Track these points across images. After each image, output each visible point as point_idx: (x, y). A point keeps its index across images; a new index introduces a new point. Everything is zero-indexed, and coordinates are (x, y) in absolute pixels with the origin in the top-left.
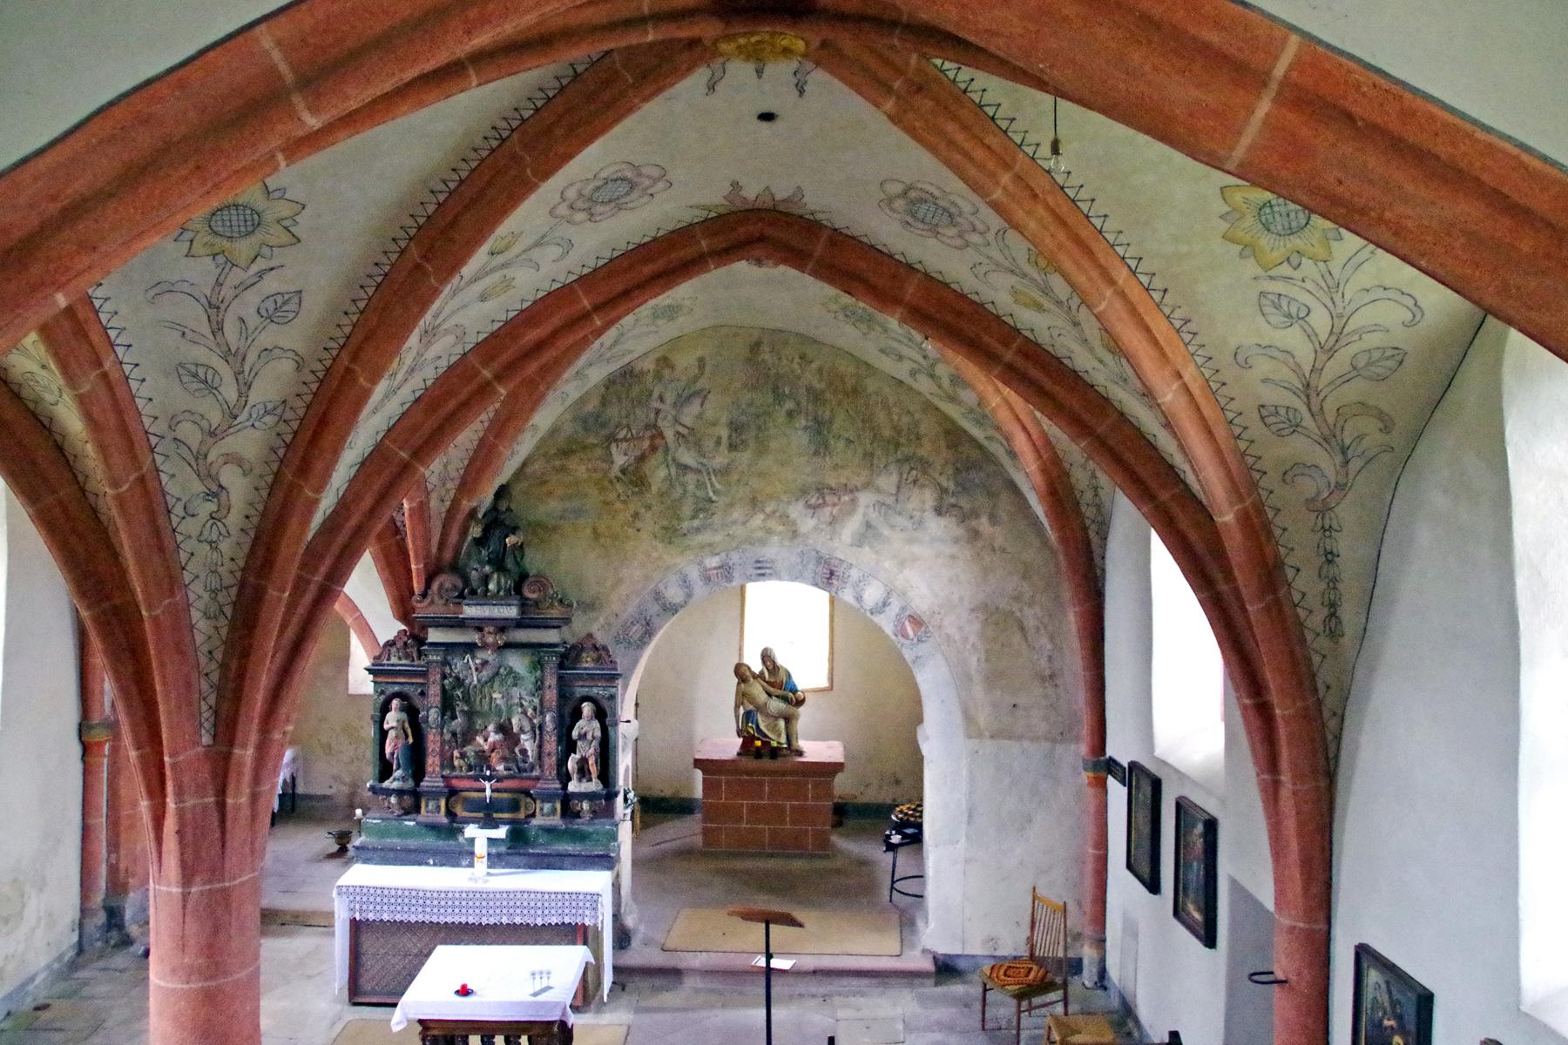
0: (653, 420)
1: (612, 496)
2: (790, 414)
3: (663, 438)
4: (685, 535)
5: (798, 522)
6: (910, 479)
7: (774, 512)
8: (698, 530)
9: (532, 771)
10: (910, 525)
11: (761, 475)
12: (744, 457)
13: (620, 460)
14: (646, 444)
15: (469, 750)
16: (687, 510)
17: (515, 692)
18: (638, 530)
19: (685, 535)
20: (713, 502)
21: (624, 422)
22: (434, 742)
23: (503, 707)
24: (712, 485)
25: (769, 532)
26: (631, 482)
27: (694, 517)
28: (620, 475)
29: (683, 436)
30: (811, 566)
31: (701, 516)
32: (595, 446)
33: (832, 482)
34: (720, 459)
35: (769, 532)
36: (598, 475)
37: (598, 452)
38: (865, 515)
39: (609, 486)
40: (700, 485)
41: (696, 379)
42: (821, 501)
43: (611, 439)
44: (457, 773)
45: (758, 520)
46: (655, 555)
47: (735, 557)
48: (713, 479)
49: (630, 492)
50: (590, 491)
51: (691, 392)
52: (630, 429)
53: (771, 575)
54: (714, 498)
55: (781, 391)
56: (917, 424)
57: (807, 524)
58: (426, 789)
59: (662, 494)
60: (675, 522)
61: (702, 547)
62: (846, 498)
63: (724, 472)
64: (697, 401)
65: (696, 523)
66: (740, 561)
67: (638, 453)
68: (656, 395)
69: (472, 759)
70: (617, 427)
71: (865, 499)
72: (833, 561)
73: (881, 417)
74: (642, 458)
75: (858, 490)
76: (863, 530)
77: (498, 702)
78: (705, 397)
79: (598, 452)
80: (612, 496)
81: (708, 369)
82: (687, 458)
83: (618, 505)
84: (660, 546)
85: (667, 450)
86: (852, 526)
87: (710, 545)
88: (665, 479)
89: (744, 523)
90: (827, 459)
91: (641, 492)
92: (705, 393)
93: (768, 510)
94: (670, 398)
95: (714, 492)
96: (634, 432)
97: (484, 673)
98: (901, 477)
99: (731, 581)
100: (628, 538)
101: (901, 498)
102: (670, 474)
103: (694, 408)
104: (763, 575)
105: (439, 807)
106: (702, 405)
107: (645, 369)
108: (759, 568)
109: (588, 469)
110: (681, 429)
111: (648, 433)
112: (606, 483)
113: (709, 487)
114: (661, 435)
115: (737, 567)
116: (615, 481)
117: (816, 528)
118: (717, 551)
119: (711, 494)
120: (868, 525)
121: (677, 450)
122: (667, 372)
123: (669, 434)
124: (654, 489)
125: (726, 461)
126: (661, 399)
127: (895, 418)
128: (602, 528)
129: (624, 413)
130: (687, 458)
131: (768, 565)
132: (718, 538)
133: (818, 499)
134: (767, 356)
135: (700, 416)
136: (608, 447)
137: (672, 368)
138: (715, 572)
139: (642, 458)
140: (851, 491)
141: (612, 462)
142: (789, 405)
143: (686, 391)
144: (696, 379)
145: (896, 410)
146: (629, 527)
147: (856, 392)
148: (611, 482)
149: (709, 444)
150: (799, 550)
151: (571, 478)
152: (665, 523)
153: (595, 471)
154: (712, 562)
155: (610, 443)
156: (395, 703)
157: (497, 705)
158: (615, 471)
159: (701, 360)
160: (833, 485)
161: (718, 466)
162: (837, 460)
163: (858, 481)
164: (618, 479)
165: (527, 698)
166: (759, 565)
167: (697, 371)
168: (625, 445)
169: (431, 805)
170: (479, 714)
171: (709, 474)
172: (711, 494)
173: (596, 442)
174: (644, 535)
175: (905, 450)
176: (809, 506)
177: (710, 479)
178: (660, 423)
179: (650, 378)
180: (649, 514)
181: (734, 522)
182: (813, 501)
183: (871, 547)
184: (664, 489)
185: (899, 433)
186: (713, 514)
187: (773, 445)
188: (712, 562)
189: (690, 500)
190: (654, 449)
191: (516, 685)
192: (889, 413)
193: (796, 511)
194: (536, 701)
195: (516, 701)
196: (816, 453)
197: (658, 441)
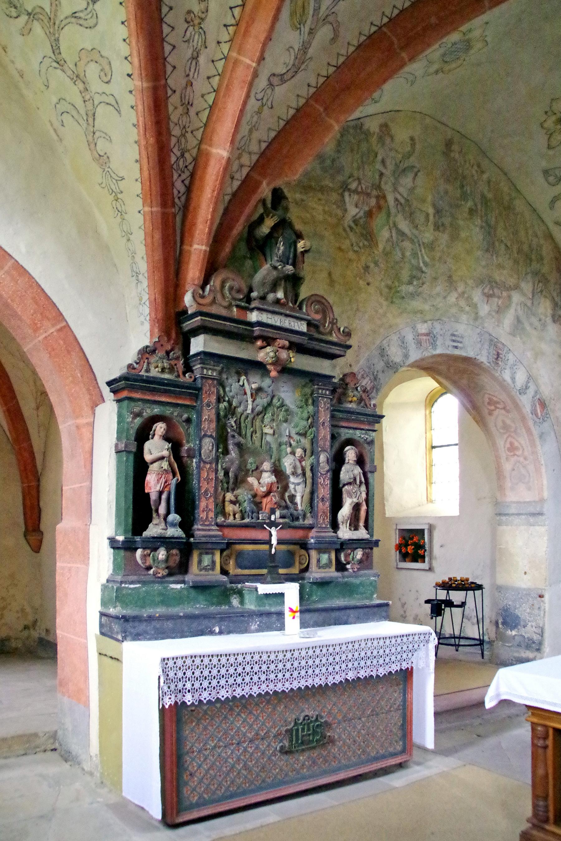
0: (377, 182)
1: (346, 244)
2: (472, 212)
3: (386, 201)
4: (403, 298)
5: (478, 305)
6: (539, 290)
7: (463, 293)
8: (413, 296)
9: (304, 520)
10: (539, 326)
11: (456, 258)
12: (444, 238)
13: (352, 211)
14: (373, 201)
15: (243, 494)
16: (405, 274)
17: (287, 429)
18: (368, 284)
19: (403, 298)
20: (423, 272)
21: (355, 174)
22: (208, 480)
23: (274, 446)
24: (423, 257)
25: (461, 310)
26: (362, 235)
27: (410, 283)
28: (353, 225)
29: (401, 204)
30: (486, 346)
31: (415, 283)
32: (332, 189)
33: (497, 278)
34: (428, 235)
35: (461, 310)
36: (333, 221)
37: (334, 196)
38: (516, 310)
39: (344, 234)
40: (415, 255)
41: (409, 155)
42: (491, 292)
43: (345, 187)
44: (231, 520)
45: (452, 298)
46: (381, 311)
47: (438, 326)
48: (423, 251)
49: (361, 244)
50: (327, 234)
51: (405, 166)
52: (360, 183)
53: (461, 348)
54: (424, 269)
55: (465, 189)
56: (541, 246)
57: (484, 309)
58: (204, 540)
59: (387, 254)
60: (397, 284)
61: (415, 312)
62: (505, 294)
63: (431, 246)
64: (411, 175)
65: (411, 289)
66: (441, 332)
67: (367, 209)
68: (380, 157)
69: (246, 504)
70: (349, 177)
71: (516, 297)
72: (499, 345)
73: (522, 233)
74: (369, 214)
75: (511, 290)
76: (516, 323)
77: (269, 438)
78: (416, 175)
79: (334, 196)
80: (346, 244)
81: (418, 147)
82: (404, 226)
83: (351, 255)
84: (385, 303)
85: (389, 214)
86: (508, 319)
87: (421, 312)
88: (388, 241)
89: (445, 298)
90: (494, 257)
91: (370, 247)
92: (416, 170)
93: (460, 290)
94: (390, 166)
95: (423, 263)
96: (364, 187)
97: (258, 400)
98: (534, 286)
99: (436, 349)
100: (360, 289)
101: (536, 303)
102: (392, 236)
103: (407, 181)
104: (456, 347)
105: (214, 562)
106: (414, 179)
107: (372, 131)
108: (454, 341)
109: (325, 212)
110: (399, 197)
111: (375, 193)
112: (341, 230)
113: (420, 257)
114: (384, 197)
115: (438, 336)
116: (348, 229)
117: (489, 314)
118: (427, 318)
119: (422, 265)
120: (518, 320)
121: (396, 216)
122: (388, 140)
123: (390, 199)
124: (381, 246)
125: (432, 238)
126: (383, 162)
127: (530, 238)
128: (337, 273)
129: (355, 165)
130: (404, 226)
131: (458, 339)
132: (427, 307)
133: (490, 289)
134: (457, 156)
135: (412, 190)
136: (342, 196)
137: (392, 138)
138: (424, 338)
139: (369, 214)
140: (508, 290)
141: (346, 210)
142: (470, 204)
143: (402, 163)
144: (409, 155)
145: (530, 232)
146: (361, 278)
147: (509, 208)
148: (345, 230)
149: (420, 218)
150: (478, 331)
151: (308, 215)
152: (389, 282)
153: (331, 215)
154: (423, 328)
155: (344, 191)
156: (160, 428)
157: (268, 443)
158: (348, 220)
159: (412, 139)
160: (498, 281)
161: (426, 241)
162: (500, 259)
163: (511, 281)
164: (351, 228)
165: (297, 437)
166: (454, 338)
167: (409, 149)
168: (356, 197)
169: (206, 560)
170: (255, 453)
171: (419, 245)
172: (422, 265)
173: (331, 185)
174: (371, 289)
175: (535, 266)
176: (484, 294)
177: (421, 251)
178: (383, 186)
179: (374, 140)
180: (376, 270)
181: (438, 294)
182: (486, 291)
183: (521, 338)
184: (388, 249)
185: (532, 251)
186: (423, 284)
187: (463, 234)
188: (423, 328)
189: (407, 266)
190: (379, 208)
191: (286, 421)
192: (527, 233)
193: (477, 296)
194: (306, 442)
195: (285, 439)
196: (487, 250)
197: (382, 202)
